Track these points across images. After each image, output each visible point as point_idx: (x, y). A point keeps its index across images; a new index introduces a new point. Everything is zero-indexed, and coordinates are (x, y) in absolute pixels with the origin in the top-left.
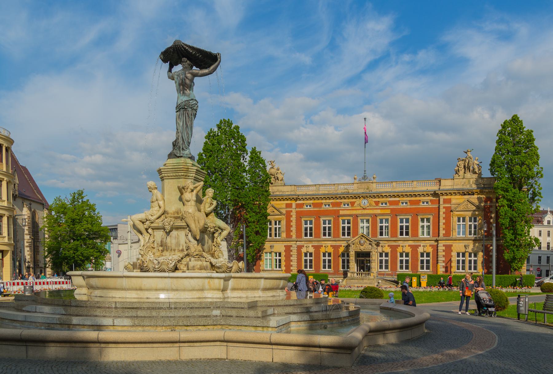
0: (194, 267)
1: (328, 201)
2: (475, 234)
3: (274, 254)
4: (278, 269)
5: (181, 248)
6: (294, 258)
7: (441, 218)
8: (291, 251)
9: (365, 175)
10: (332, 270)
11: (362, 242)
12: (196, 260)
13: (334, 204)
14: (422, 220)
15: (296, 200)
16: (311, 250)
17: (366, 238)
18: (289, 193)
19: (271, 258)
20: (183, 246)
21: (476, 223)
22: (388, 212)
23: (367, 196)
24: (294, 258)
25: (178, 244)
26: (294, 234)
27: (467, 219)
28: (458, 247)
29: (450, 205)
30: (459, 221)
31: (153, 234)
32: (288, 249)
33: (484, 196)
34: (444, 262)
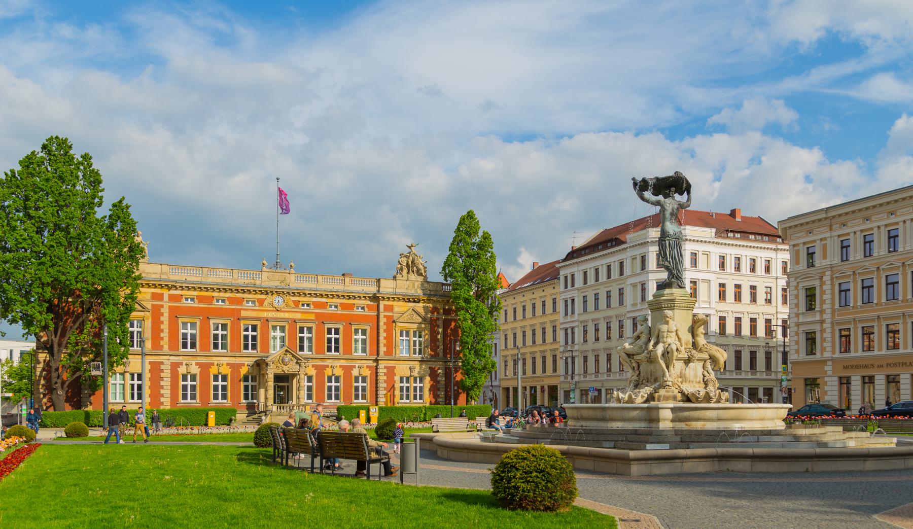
1: (222, 294)
2: (420, 353)
3: (128, 376)
4: (136, 400)
6: (166, 383)
7: (381, 331)
8: (162, 371)
9: (278, 261)
10: (229, 402)
11: (287, 359)
13: (232, 301)
14: (356, 331)
15: (169, 288)
16: (195, 370)
17: (292, 354)
18: (158, 276)
19: (123, 382)
21: (421, 339)
22: (312, 317)
23: (283, 292)
24: (166, 383)
26: (165, 343)
27: (411, 333)
28: (402, 369)
29: (391, 314)
30: (402, 335)
32: (156, 368)
33: (431, 306)
34: (385, 389)
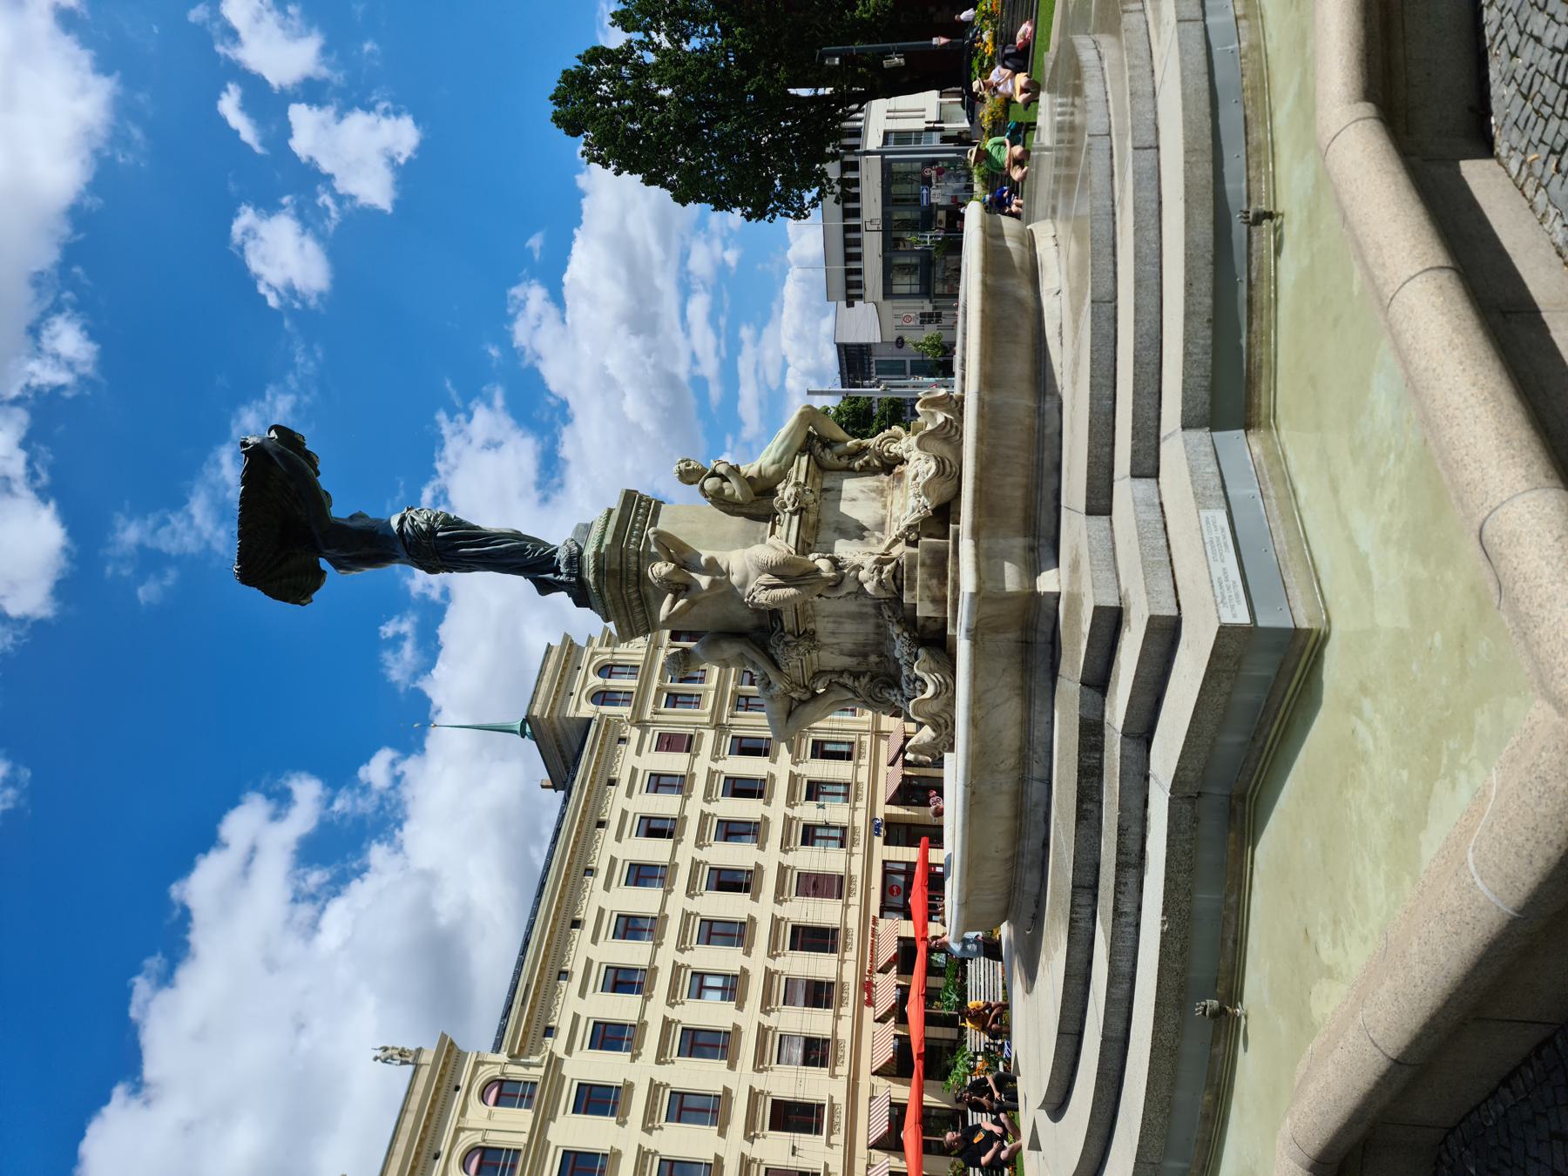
0: (934, 600)
5: (871, 610)
12: (912, 588)
20: (864, 605)
25: (859, 617)
31: (829, 677)
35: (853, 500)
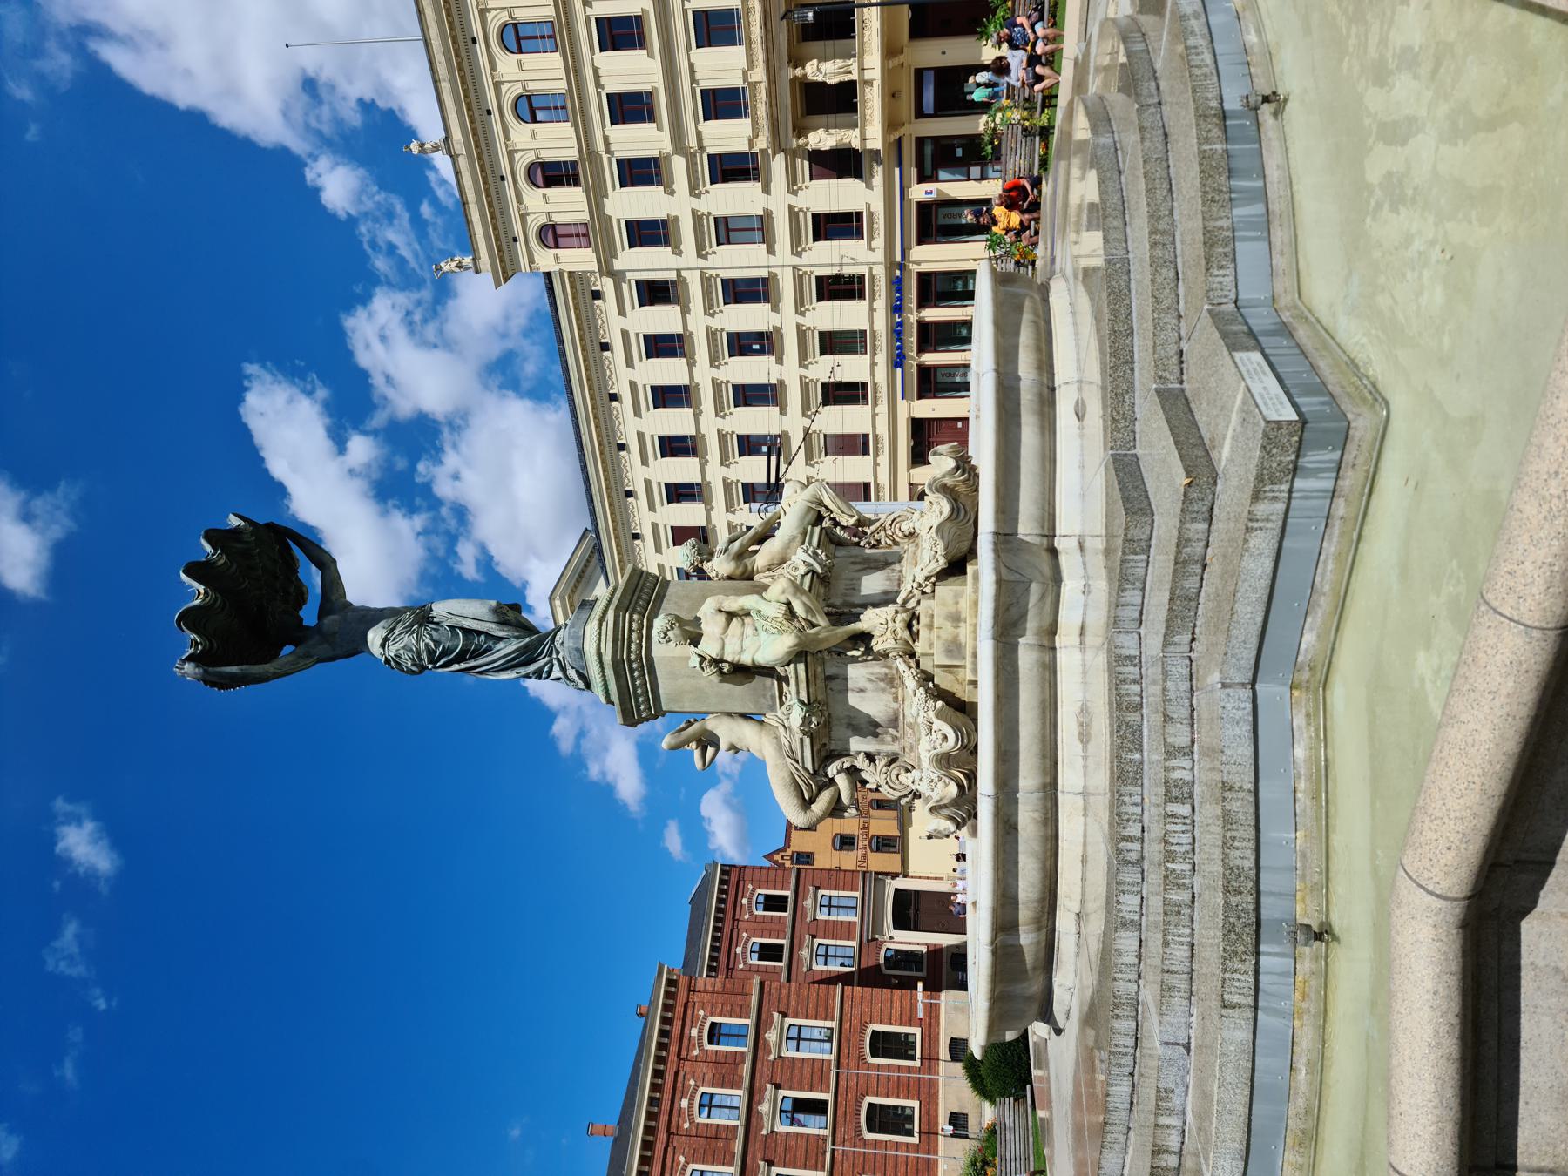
35: (862, 690)
